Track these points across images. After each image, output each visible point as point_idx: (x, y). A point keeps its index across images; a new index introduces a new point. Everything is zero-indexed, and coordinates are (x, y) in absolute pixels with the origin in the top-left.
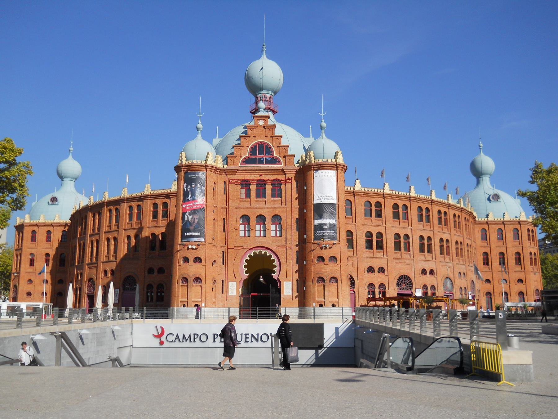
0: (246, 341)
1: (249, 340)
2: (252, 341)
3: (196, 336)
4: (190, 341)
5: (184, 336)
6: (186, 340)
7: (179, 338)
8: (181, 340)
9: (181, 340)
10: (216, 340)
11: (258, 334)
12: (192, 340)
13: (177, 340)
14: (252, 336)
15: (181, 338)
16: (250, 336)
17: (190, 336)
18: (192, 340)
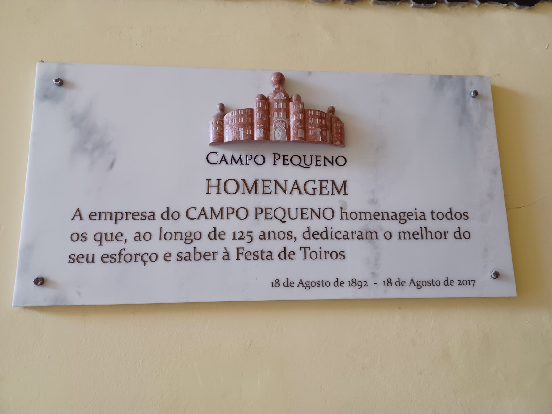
0: (317, 165)
1: (322, 162)
2: (325, 165)
3: (249, 157)
4: (241, 164)
5: (232, 157)
6: (236, 163)
7: (225, 160)
8: (229, 162)
9: (229, 162)
10: (277, 162)
11: (333, 157)
12: (244, 161)
13: (224, 163)
14: (325, 158)
15: (229, 159)
16: (322, 159)
17: (240, 157)
18: (244, 161)
